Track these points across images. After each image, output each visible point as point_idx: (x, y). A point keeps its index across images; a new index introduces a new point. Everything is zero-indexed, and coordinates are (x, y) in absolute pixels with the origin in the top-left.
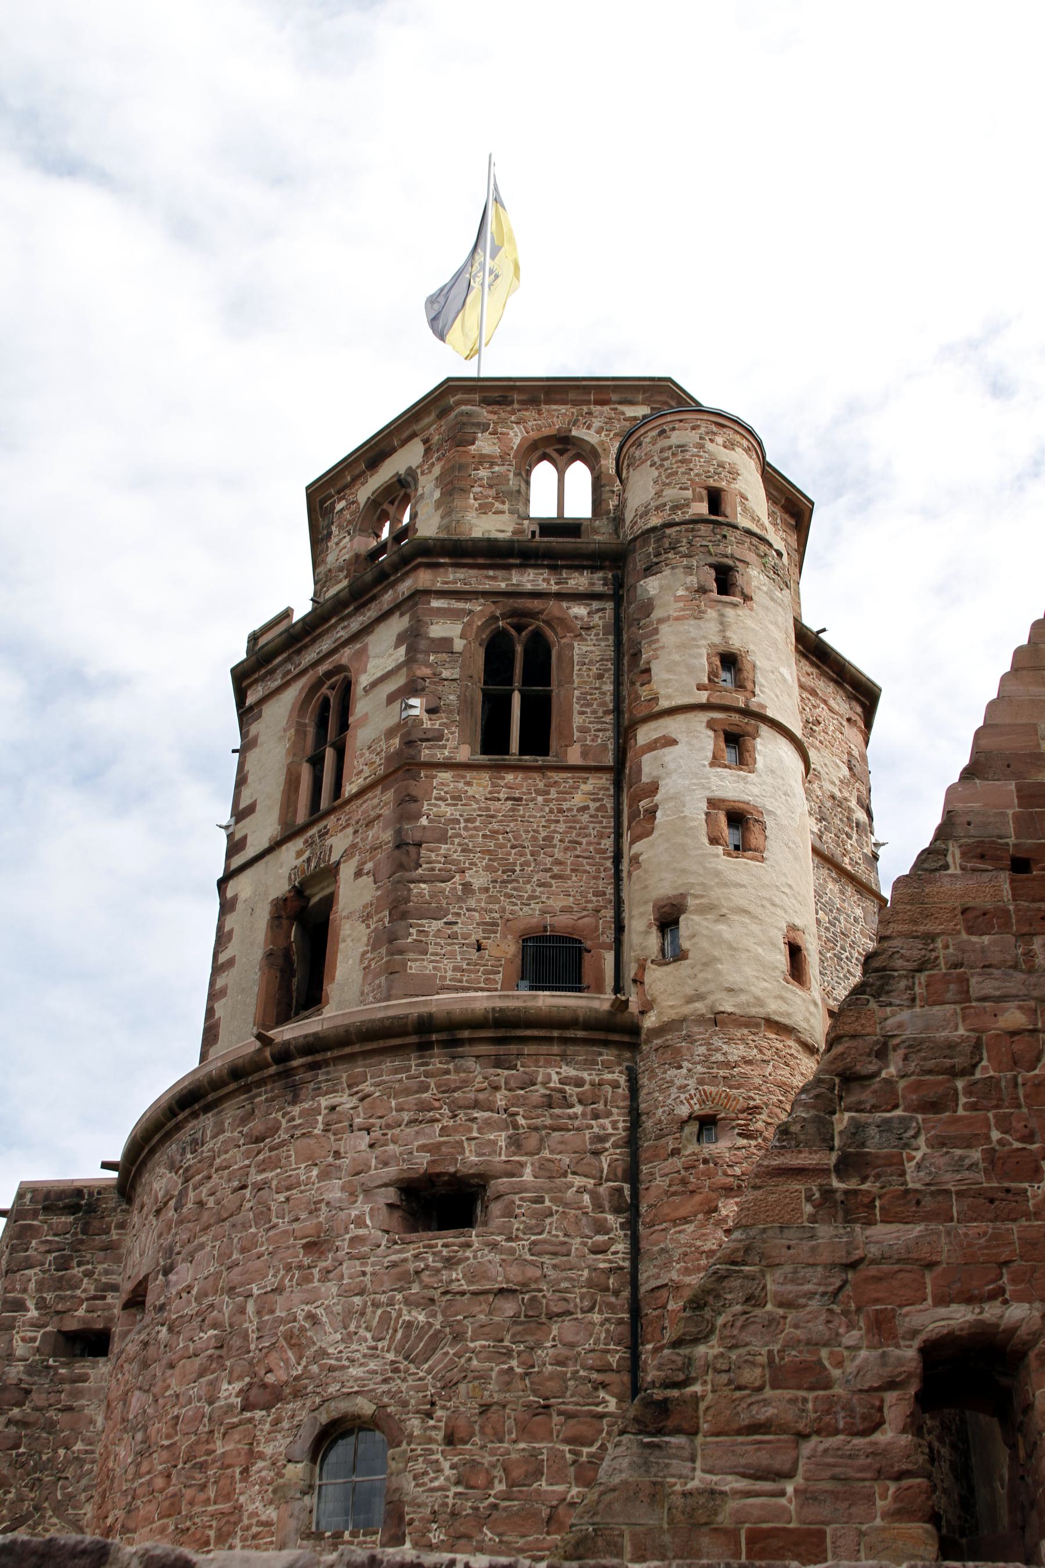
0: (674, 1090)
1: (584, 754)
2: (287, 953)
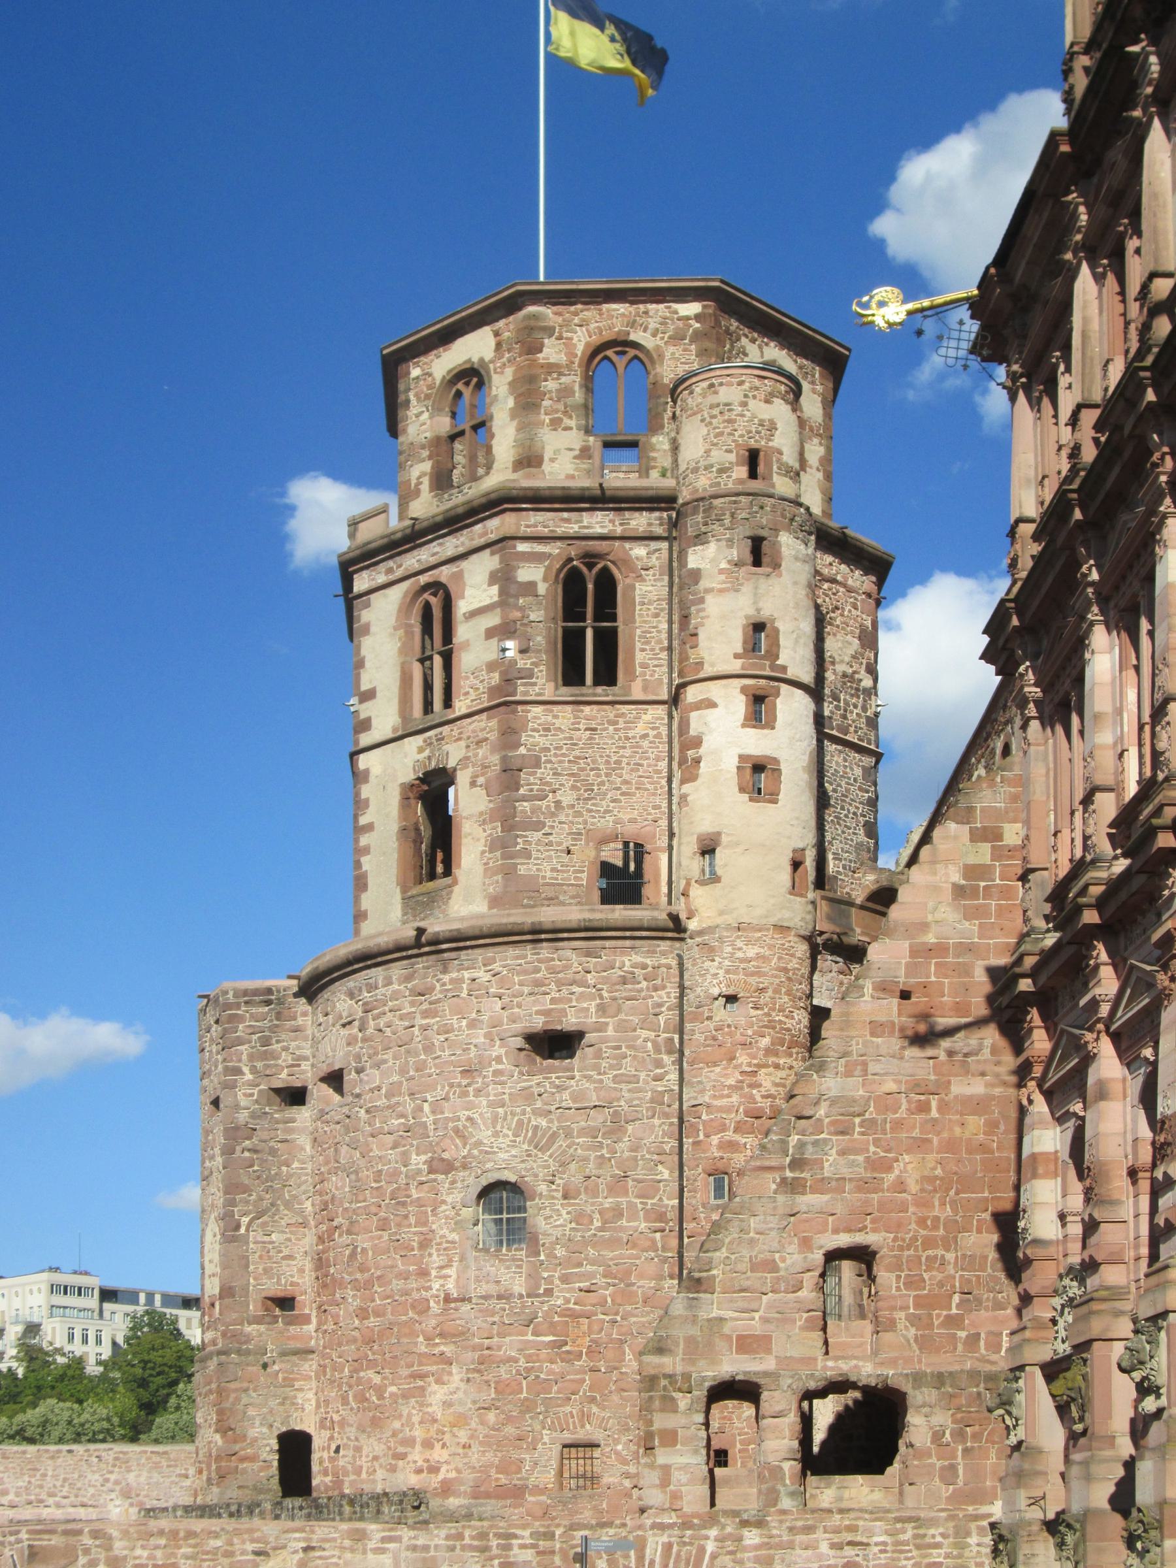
0: (709, 976)
1: (645, 689)
2: (416, 824)
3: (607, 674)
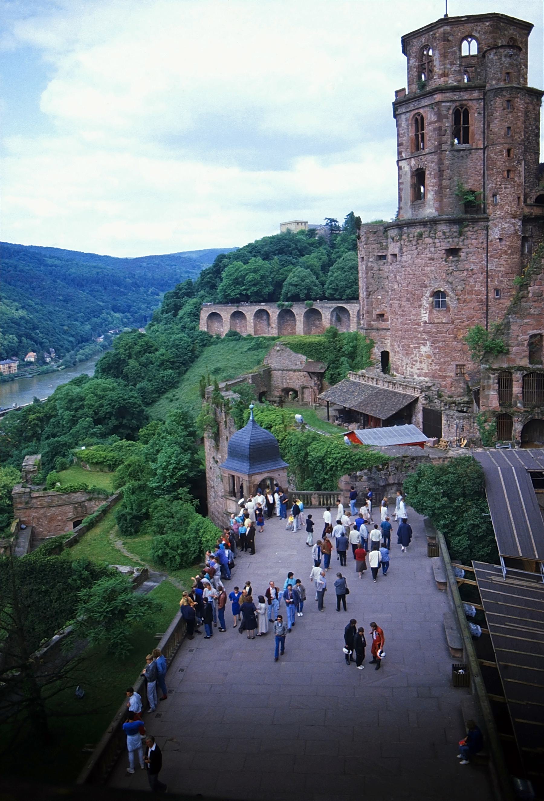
3: (466, 141)
